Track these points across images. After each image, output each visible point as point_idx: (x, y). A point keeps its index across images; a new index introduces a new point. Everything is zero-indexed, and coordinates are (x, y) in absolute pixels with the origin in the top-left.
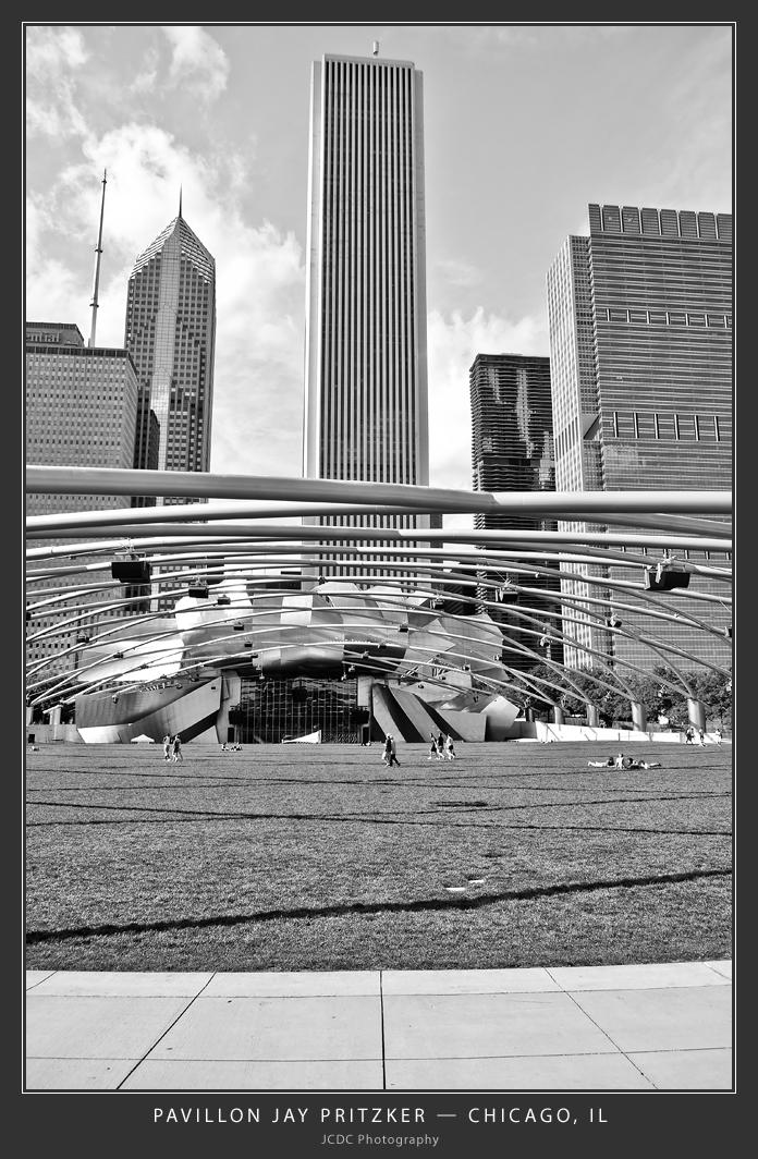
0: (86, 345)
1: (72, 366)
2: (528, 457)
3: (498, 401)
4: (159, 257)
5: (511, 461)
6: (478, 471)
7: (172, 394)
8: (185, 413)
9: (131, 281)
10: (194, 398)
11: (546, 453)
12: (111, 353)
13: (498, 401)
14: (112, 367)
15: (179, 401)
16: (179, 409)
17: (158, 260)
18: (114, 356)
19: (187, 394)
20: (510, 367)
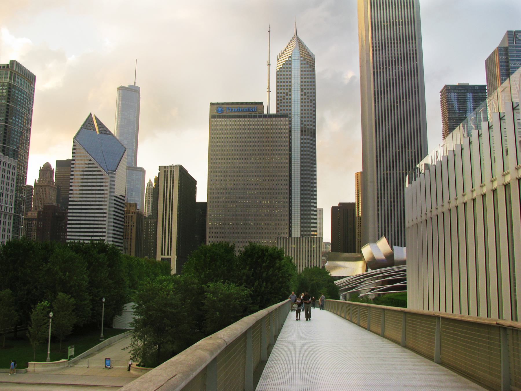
1: (264, 123)
3: (457, 110)
4: (290, 59)
7: (302, 128)
8: (308, 137)
9: (278, 71)
10: (311, 129)
13: (457, 110)
15: (305, 131)
16: (305, 135)
17: (290, 61)
18: (282, 117)
20: (463, 91)
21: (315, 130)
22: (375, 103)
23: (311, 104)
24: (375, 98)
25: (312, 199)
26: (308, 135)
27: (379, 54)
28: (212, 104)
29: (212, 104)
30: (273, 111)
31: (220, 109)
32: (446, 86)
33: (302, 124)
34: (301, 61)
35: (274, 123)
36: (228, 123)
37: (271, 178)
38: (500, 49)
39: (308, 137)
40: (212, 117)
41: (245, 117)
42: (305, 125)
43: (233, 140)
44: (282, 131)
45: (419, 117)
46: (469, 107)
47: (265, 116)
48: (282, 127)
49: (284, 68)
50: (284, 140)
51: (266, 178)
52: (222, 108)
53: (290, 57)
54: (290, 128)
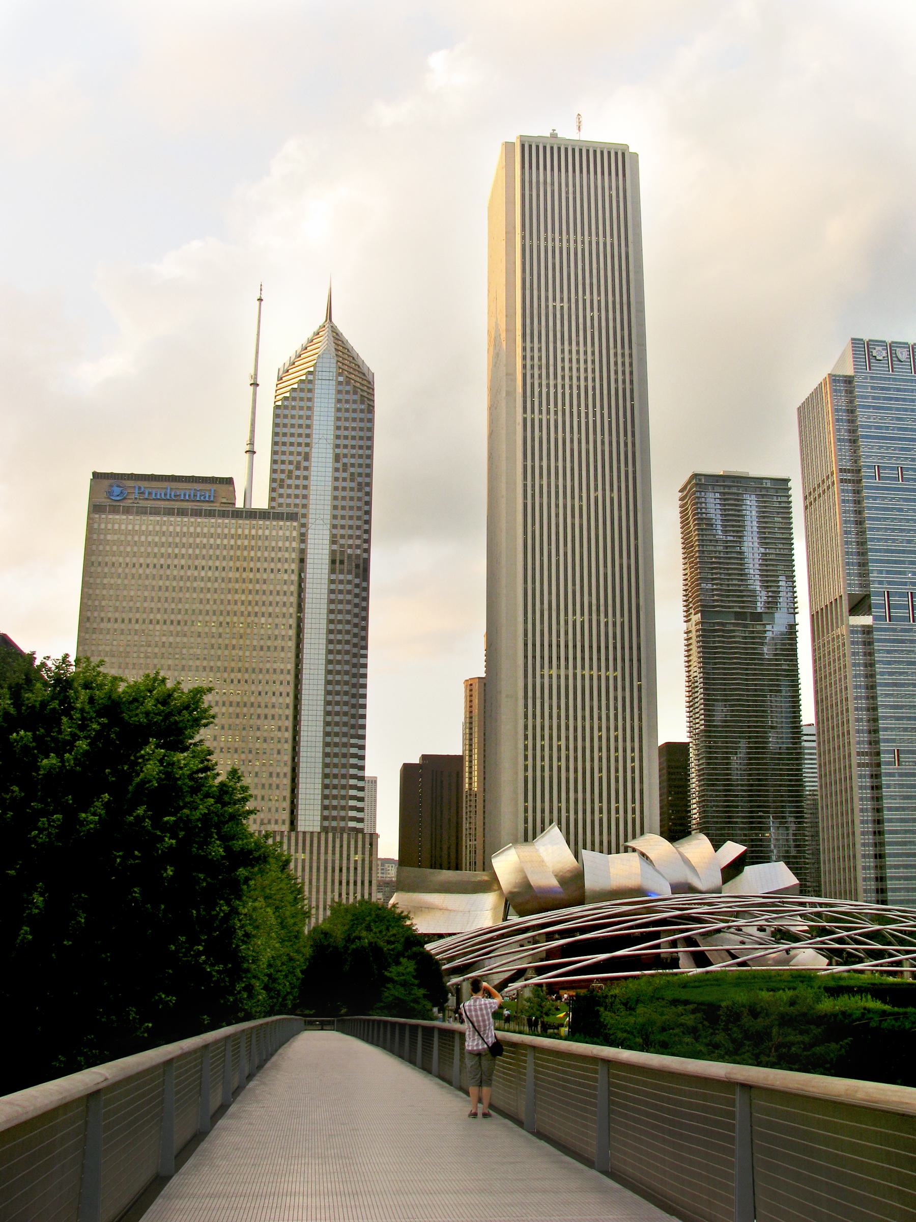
0: (239, 504)
1: (233, 531)
2: (759, 610)
4: (310, 377)
5: (738, 615)
7: (333, 553)
8: (350, 577)
9: (277, 407)
10: (358, 556)
15: (342, 562)
16: (342, 572)
17: (310, 382)
18: (282, 519)
19: (349, 551)
20: (734, 490)
21: (367, 562)
22: (525, 497)
23: (360, 494)
24: (525, 486)
25: (353, 737)
26: (349, 572)
27: (540, 376)
28: (96, 475)
29: (96, 475)
30: (261, 501)
31: (117, 490)
32: (695, 476)
33: (333, 542)
34: (340, 383)
35: (260, 532)
37: (246, 676)
38: (834, 381)
39: (350, 577)
40: (95, 508)
41: (182, 513)
42: (342, 546)
43: (148, 571)
44: (280, 555)
45: (636, 538)
46: (748, 528)
47: (237, 514)
48: (280, 544)
49: (294, 399)
50: (286, 577)
51: (232, 676)
52: (125, 488)
53: (310, 373)
54: (303, 551)
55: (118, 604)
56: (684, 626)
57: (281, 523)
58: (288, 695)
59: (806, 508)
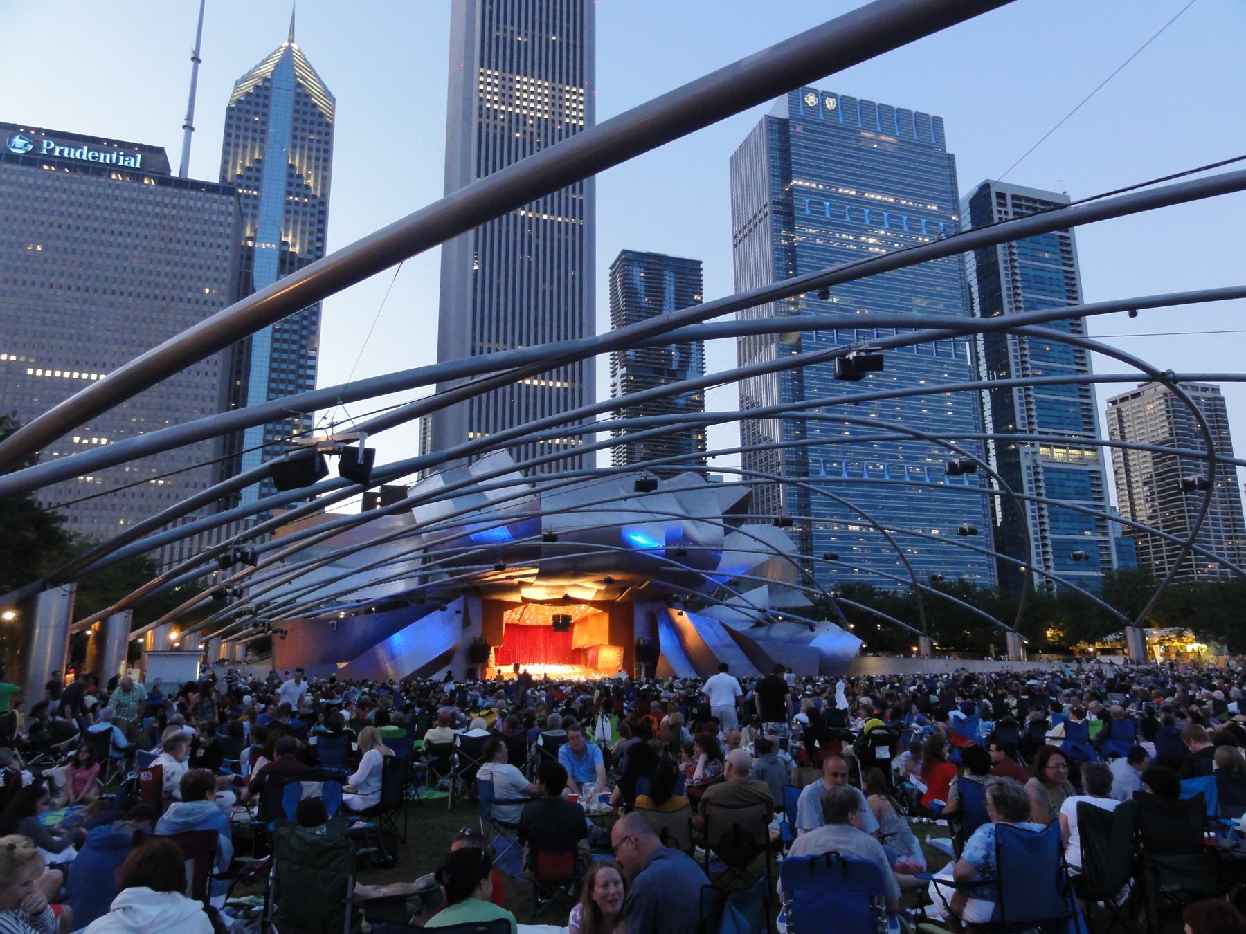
1: (159, 199)
4: (268, 84)
6: (618, 379)
9: (230, 109)
11: (693, 365)
12: (211, 188)
14: (215, 206)
17: (267, 89)
32: (624, 252)
36: (40, 182)
43: (51, 231)
44: (213, 229)
46: (667, 299)
48: (214, 218)
50: (219, 252)
55: (9, 263)
56: (611, 381)
57: (216, 196)
58: (215, 375)
59: (735, 246)
